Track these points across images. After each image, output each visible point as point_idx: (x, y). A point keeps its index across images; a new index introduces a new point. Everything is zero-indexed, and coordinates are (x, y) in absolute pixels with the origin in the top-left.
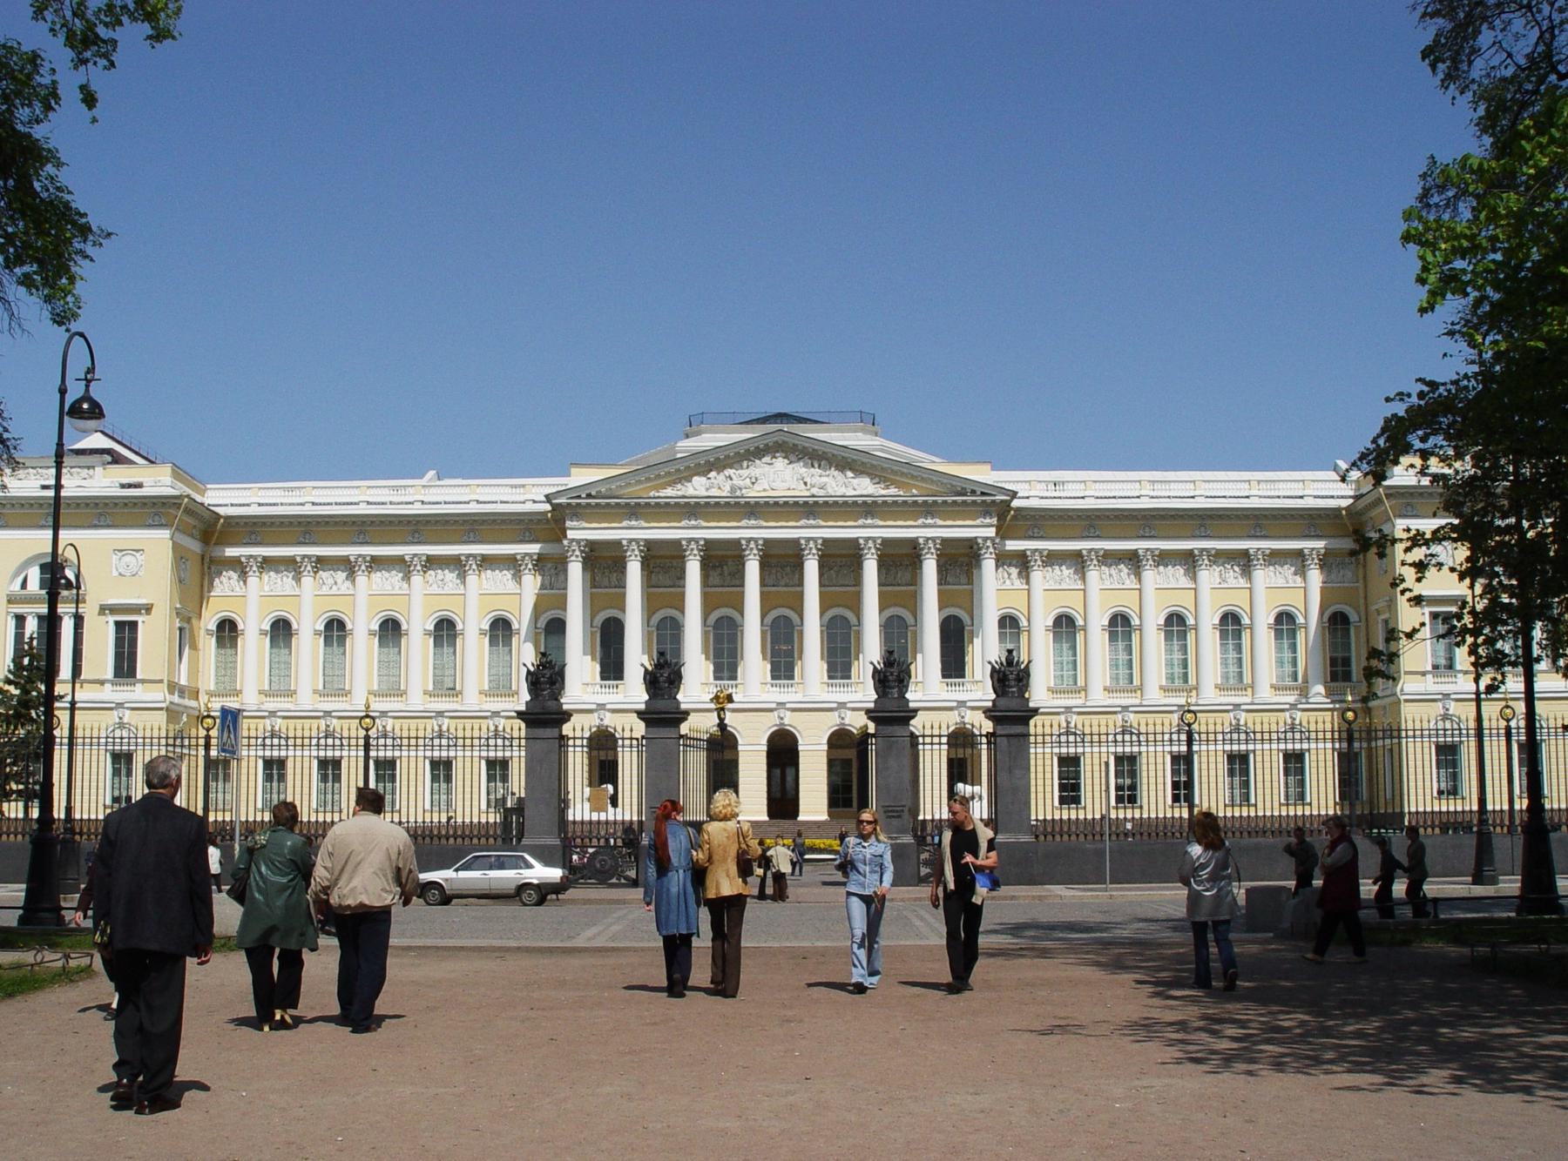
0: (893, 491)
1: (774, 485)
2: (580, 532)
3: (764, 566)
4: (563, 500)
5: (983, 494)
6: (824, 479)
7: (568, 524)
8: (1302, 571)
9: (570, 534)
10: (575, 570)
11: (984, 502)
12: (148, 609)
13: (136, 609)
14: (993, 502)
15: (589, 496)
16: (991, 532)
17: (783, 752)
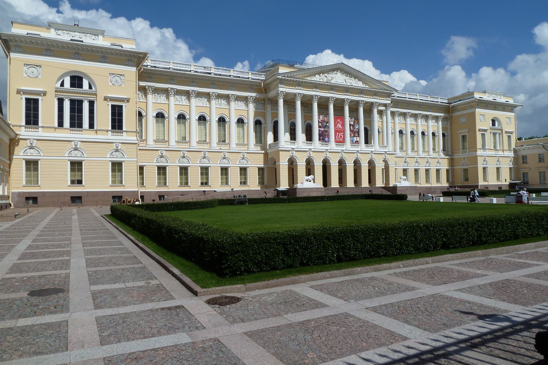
0: (367, 87)
2: (283, 89)
8: (437, 121)
12: (128, 100)
13: (122, 100)
16: (390, 102)
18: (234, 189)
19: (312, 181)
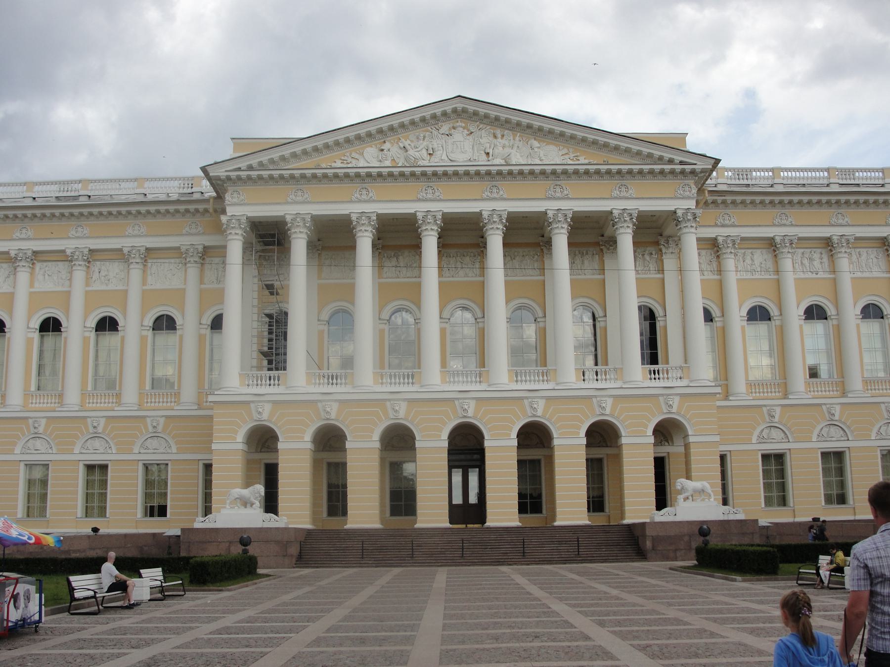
1: (453, 156)
3: (443, 246)
4: (219, 172)
5: (681, 163)
6: (507, 150)
7: (228, 197)
9: (230, 211)
10: (235, 249)
11: (683, 172)
14: (693, 172)
15: (250, 168)
16: (692, 204)
17: (467, 449)
18: (102, 531)
19: (257, 504)
